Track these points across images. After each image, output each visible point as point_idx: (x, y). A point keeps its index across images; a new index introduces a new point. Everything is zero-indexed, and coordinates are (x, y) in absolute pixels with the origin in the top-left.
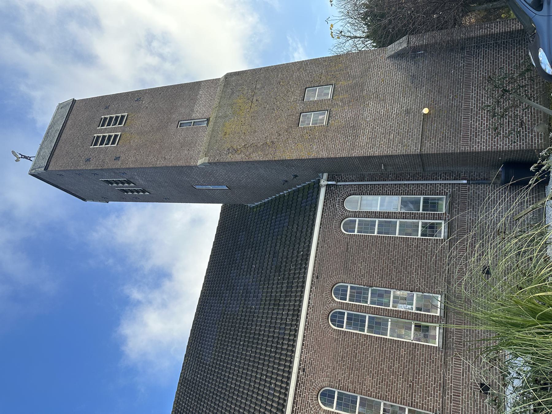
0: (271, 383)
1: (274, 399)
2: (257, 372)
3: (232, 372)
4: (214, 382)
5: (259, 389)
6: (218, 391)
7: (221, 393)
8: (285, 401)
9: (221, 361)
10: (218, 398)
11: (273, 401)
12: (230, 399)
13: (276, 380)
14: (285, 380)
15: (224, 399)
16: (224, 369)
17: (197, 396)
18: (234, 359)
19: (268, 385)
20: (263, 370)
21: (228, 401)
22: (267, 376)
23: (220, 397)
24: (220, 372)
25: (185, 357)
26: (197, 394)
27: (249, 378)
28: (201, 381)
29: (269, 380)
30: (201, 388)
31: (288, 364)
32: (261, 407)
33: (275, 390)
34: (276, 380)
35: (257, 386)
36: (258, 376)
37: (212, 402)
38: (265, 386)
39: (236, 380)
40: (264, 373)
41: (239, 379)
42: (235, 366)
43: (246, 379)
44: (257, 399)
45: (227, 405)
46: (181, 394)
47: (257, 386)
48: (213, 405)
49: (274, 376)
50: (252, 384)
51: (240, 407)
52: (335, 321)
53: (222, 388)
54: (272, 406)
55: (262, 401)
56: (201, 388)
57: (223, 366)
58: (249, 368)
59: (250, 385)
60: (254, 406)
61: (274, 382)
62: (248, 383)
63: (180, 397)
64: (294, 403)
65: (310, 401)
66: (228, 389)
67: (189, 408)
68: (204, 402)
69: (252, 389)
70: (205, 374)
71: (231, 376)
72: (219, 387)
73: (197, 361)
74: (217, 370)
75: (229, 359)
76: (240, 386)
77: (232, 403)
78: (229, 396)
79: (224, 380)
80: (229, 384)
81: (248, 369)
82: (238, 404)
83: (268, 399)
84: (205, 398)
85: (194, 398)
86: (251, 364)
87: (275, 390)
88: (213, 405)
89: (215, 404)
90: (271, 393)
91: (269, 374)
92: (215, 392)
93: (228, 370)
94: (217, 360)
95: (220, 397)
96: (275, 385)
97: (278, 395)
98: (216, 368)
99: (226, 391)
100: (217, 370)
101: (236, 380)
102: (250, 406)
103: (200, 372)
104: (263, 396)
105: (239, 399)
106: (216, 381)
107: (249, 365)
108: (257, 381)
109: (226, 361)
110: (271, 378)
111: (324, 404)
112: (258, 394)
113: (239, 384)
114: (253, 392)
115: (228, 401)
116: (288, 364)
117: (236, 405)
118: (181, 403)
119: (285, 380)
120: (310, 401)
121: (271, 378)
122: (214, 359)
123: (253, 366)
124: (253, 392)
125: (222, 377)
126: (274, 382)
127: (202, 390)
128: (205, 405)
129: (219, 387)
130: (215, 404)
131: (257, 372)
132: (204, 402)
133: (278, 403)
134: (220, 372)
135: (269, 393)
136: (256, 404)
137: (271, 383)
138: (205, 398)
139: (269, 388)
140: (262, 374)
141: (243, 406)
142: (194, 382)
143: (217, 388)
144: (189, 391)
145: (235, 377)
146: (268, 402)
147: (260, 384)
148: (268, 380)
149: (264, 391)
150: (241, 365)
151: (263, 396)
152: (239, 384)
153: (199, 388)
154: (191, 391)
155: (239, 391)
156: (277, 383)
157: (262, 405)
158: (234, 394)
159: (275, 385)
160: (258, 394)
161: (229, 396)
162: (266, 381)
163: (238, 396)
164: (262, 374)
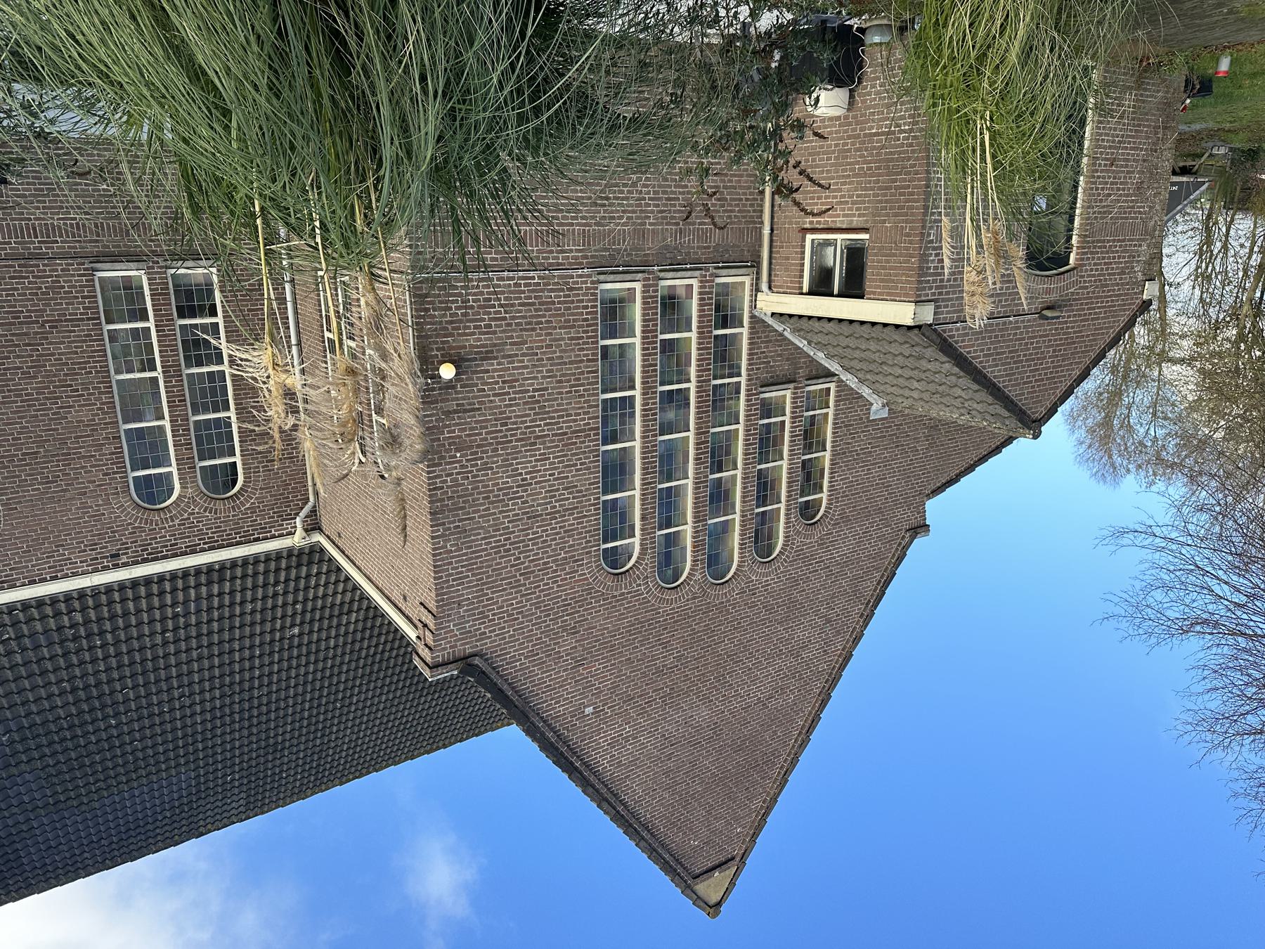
0: (176, 616)
1: (204, 595)
2: (166, 656)
3: (188, 712)
4: (228, 738)
5: (199, 636)
6: (241, 720)
8: (198, 571)
10: (255, 712)
11: (210, 596)
12: (246, 686)
13: (163, 607)
14: (155, 589)
15: (251, 698)
16: (189, 730)
17: (270, 758)
18: (157, 720)
19: (182, 620)
20: (153, 646)
21: (251, 688)
22: (164, 632)
23: (251, 708)
24: (199, 738)
25: (202, 834)
27: (185, 667)
28: (237, 768)
30: (251, 759)
32: (232, 616)
33: (186, 602)
35: (194, 643)
36: (172, 649)
37: (269, 720)
38: (187, 626)
39: (202, 692)
40: (159, 639)
42: (172, 710)
43: (190, 673)
44: (221, 631)
45: (261, 686)
46: (282, 795)
47: (194, 643)
48: (273, 716)
50: (195, 654)
51: (252, 657)
53: (232, 713)
54: (220, 594)
55: (221, 619)
56: (251, 759)
59: (200, 658)
60: (237, 631)
61: (169, 610)
62: (196, 665)
64: (194, 552)
65: (177, 522)
66: (227, 701)
67: (301, 762)
68: (276, 735)
69: (205, 651)
71: (198, 709)
72: (233, 722)
73: (202, 802)
74: (200, 746)
75: (164, 732)
76: (211, 679)
77: (252, 678)
78: (242, 691)
79: (214, 718)
80: (218, 703)
82: (247, 664)
83: (210, 609)
84: (268, 738)
85: (278, 762)
87: (186, 602)
88: (273, 716)
89: (269, 712)
91: (158, 627)
92: (246, 724)
93: (189, 721)
94: (177, 757)
95: (251, 708)
96: (174, 605)
97: (192, 592)
100: (200, 746)
101: (202, 692)
103: (220, 782)
104: (210, 621)
105: (237, 667)
106: (224, 734)
107: (157, 681)
108: (184, 648)
109: (170, 737)
110: (164, 619)
112: (210, 633)
114: (210, 645)
115: (251, 688)
117: (252, 668)
118: (298, 784)
120: (177, 522)
121: (164, 619)
122: (178, 765)
123: (156, 670)
124: (210, 645)
125: (209, 726)
126: (169, 610)
127: (254, 755)
128: (281, 731)
129: (233, 722)
130: (269, 712)
131: (166, 656)
132: (276, 735)
133: (210, 583)
134: (199, 738)
135: (198, 611)
136: (232, 628)
137: (176, 616)
138: (268, 738)
139: (187, 614)
140: (165, 643)
143: (237, 726)
144: (269, 780)
145: (198, 698)
147: (187, 638)
149: (198, 624)
150: (165, 697)
151: (210, 621)
152: (207, 684)
153: (254, 763)
154: (266, 776)
155: (221, 676)
156: (169, 602)
157: (227, 615)
158: (232, 684)
159: (174, 605)
160: (210, 633)
161: (242, 691)
162: (176, 629)
163: (232, 673)
164: (165, 643)
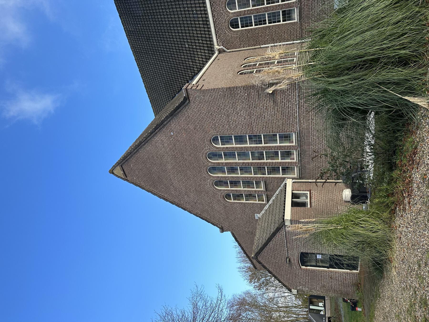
0: (193, 11)
1: (199, 19)
2: (180, 8)
3: (162, 14)
4: (152, 25)
5: (186, 17)
6: (158, 29)
7: (161, 30)
8: (207, 18)
9: (150, 10)
10: (161, 34)
11: (199, 21)
12: (170, 31)
13: (196, 7)
14: (202, 5)
15: (165, 32)
16: (155, 14)
17: (145, 38)
18: (159, 5)
19: (191, 13)
20: (183, 4)
21: (168, 32)
22: (188, 7)
23: (162, 32)
24: (153, 17)
25: (120, 17)
26: (144, 37)
27: (176, 13)
28: (142, 28)
29: (191, 9)
30: (145, 32)
31: (202, 9)
32: (192, 27)
33: (197, 14)
34: (196, 7)
35: (184, 16)
36: (182, 9)
37: (158, 37)
38: (189, 14)
39: (168, 18)
40: (185, 6)
41: (169, 16)
42: (162, 9)
43: (174, 15)
44: (187, 24)
45: (169, 35)
46: (132, 41)
47: (184, 16)
48: (159, 39)
49: (193, 6)
50: (180, 16)
51: (178, 33)
52: (233, 25)
53: (160, 27)
54: (199, 24)
55: (191, 24)
56: (145, 32)
57: (154, 13)
58: (173, 7)
59: (179, 18)
60: (187, 29)
61: (195, 9)
62: (177, 16)
63: (133, 43)
64: (213, 17)
65: (222, 12)
66: (165, 25)
67: (143, 47)
68: (153, 40)
69: (181, 19)
70: (143, 23)
71: (162, 17)
72: (158, 27)
73: (131, 17)
74: (150, 17)
75: (155, 6)
76: (172, 21)
77: (172, 33)
78: (168, 30)
79: (159, 21)
80: (164, 22)
81: (173, 8)
82: (176, 31)
83: (195, 21)
84: (152, 37)
85: (144, 40)
86: (173, 3)
87: (197, 14)
88: (159, 39)
89: (161, 38)
90: (195, 17)
91: (189, 6)
92: (157, 31)
93: (158, 14)
94: (147, 10)
95: (162, 32)
96: (196, 10)
97: (200, 16)
98: (149, 16)
99: (164, 27)
100: (150, 17)
101: (168, 18)
102: (185, 30)
103: (138, 23)
104: (191, 21)
105: (176, 28)
106: (154, 24)
107: (172, 5)
108: (182, 13)
109: (153, 8)
110: (192, 7)
111: (231, 9)
112: (187, 21)
113: (171, 19)
114: (183, 21)
115: (168, 32)
116: (202, 9)
117: (175, 33)
118: (136, 46)
119: (202, 5)
120: (222, 12)
121: (192, 7)
122: (144, 10)
123: (176, 5)
124: (183, 21)
125: (157, 20)
126: (195, 9)
127: (146, 33)
128: (154, 41)
129: (158, 27)
130: (161, 38)
131: (180, 8)
132: (153, 40)
133: (203, 21)
134: (153, 17)
135: (194, 17)
136: (188, 27)
137: (193, 11)
138: (152, 37)
139: (193, 14)
140: (184, 8)
141: (180, 31)
142: (138, 30)
143: (156, 28)
144: (138, 37)
145: (166, 17)
146: (196, 22)
147: (185, 14)
148: (190, 9)
149: (190, 17)
150: (167, 7)
151: (191, 21)
152: (171, 19)
153: (144, 33)
154: (139, 36)
155: (173, 24)
156: (197, 9)
157: (193, 26)
158: (170, 27)
159: (196, 10)
160: (187, 21)
161: (168, 30)
162: (188, 11)
163: (174, 27)
164: (184, 8)
